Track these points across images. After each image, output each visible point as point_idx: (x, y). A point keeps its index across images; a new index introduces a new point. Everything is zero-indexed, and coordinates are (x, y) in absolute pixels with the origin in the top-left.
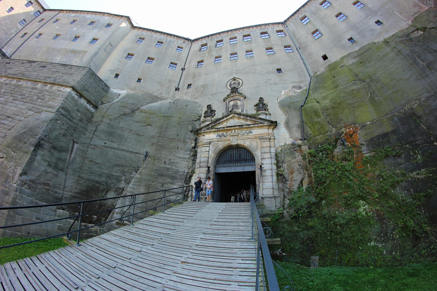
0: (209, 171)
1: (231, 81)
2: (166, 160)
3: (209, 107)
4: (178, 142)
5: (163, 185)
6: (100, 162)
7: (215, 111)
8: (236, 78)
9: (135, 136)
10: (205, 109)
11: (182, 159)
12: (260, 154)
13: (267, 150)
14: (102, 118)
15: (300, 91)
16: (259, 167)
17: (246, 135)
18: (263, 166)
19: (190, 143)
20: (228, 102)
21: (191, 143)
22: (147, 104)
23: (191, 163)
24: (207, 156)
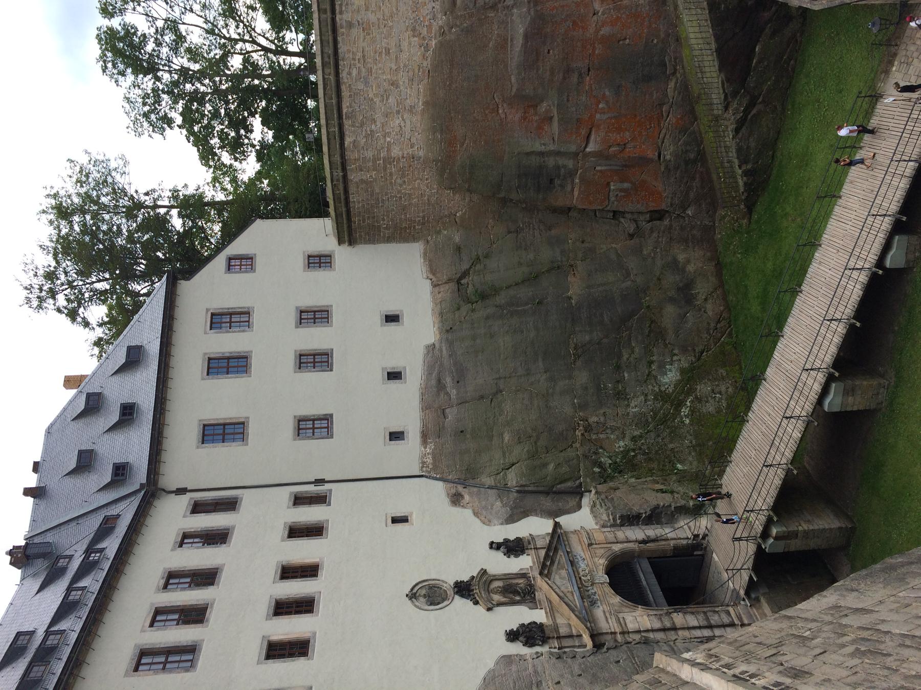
3: (512, 636)
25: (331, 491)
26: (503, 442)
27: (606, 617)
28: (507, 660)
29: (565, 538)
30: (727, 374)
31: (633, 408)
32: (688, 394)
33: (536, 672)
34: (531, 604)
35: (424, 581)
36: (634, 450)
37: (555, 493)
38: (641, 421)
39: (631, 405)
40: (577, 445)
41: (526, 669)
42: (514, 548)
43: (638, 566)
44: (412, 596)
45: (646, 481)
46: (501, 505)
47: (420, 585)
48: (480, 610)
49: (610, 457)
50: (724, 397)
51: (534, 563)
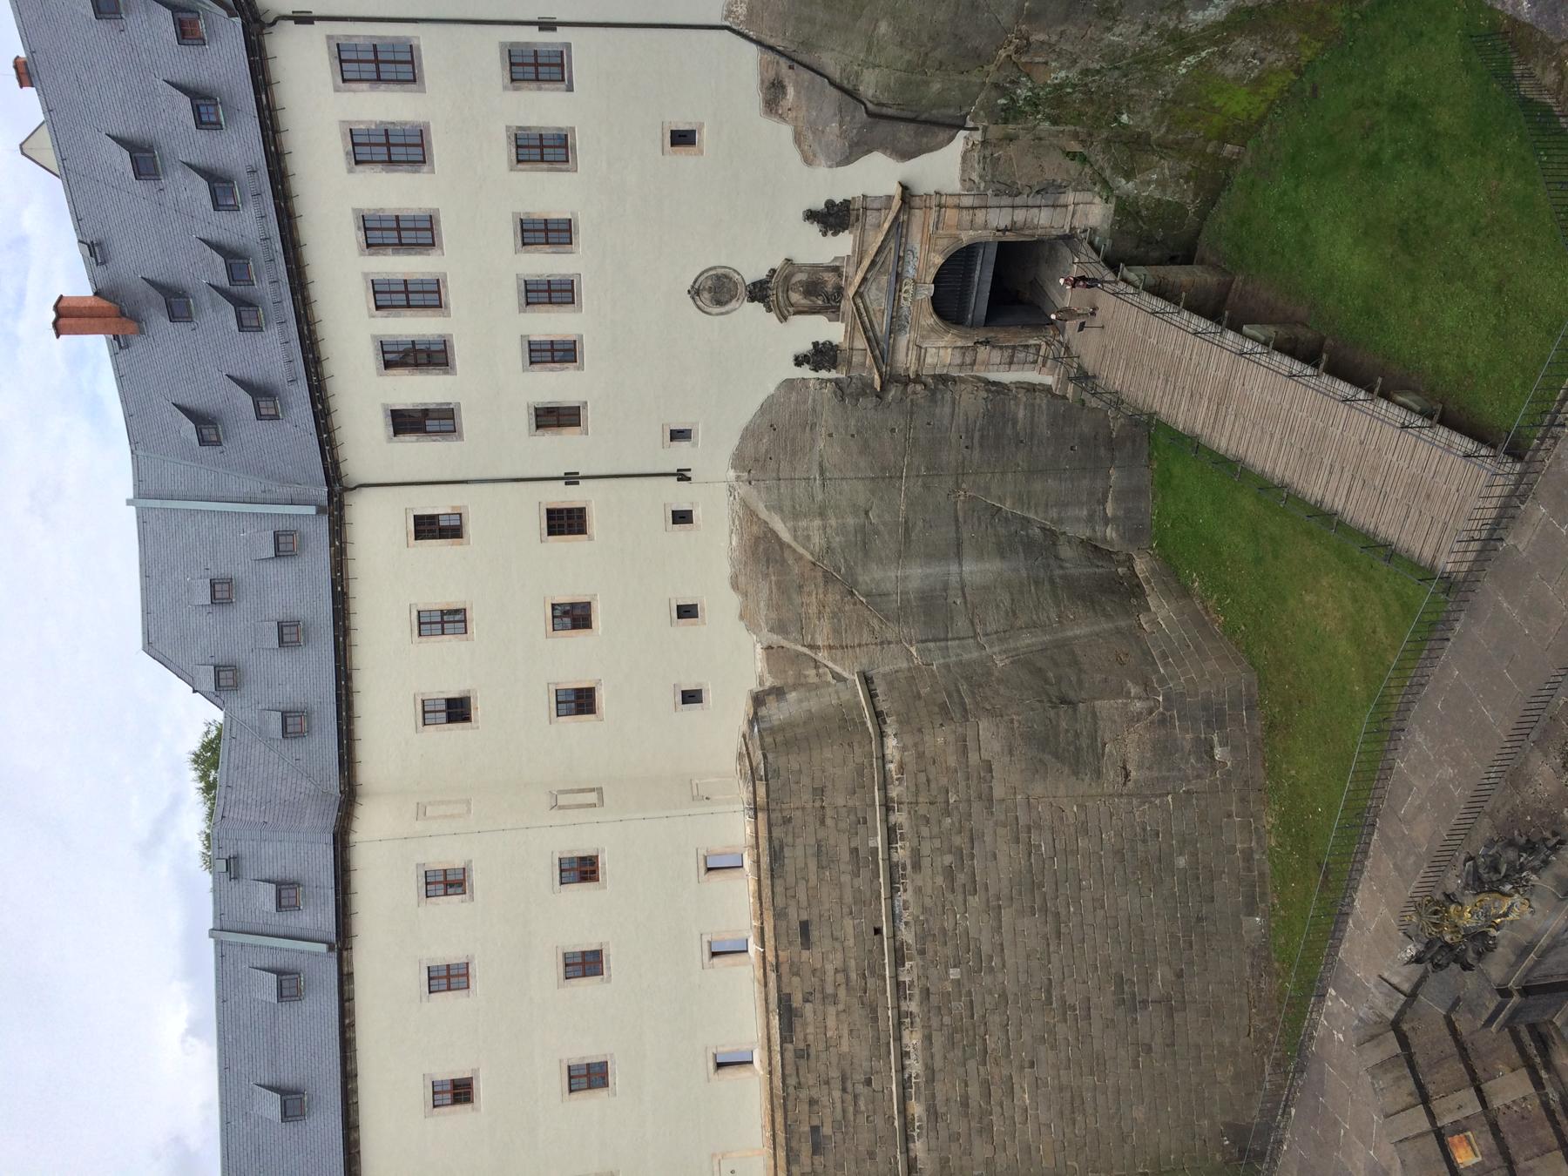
0: (986, 343)
1: (699, 303)
2: (963, 446)
3: (799, 361)
4: (915, 428)
5: (1022, 442)
6: (1008, 596)
7: (815, 344)
8: (693, 287)
9: (914, 537)
10: (806, 372)
11: (957, 409)
12: (971, 233)
13: (966, 215)
14: (889, 643)
15: (791, 91)
16: (1000, 233)
17: (917, 264)
18: (1002, 226)
19: (915, 397)
20: (791, 309)
21: (914, 393)
22: (789, 546)
23: (963, 386)
24: (949, 350)
25: (568, 46)
26: (875, 29)
27: (908, 349)
28: (789, 384)
29: (905, 231)
30: (1297, 44)
31: (1114, 35)
32: (1216, 44)
33: (814, 410)
34: (832, 316)
35: (711, 269)
36: (1074, 86)
37: (925, 122)
38: (1114, 57)
39: (1115, 29)
40: (992, 68)
41: (805, 402)
42: (833, 217)
43: (981, 251)
44: (695, 292)
45: (1063, 132)
46: (837, 131)
47: (706, 275)
48: (773, 316)
49: (1030, 89)
50: (1260, 68)
51: (854, 251)
